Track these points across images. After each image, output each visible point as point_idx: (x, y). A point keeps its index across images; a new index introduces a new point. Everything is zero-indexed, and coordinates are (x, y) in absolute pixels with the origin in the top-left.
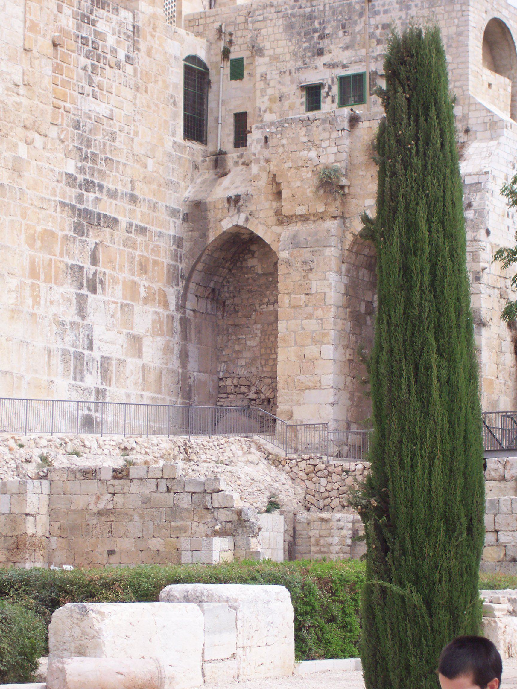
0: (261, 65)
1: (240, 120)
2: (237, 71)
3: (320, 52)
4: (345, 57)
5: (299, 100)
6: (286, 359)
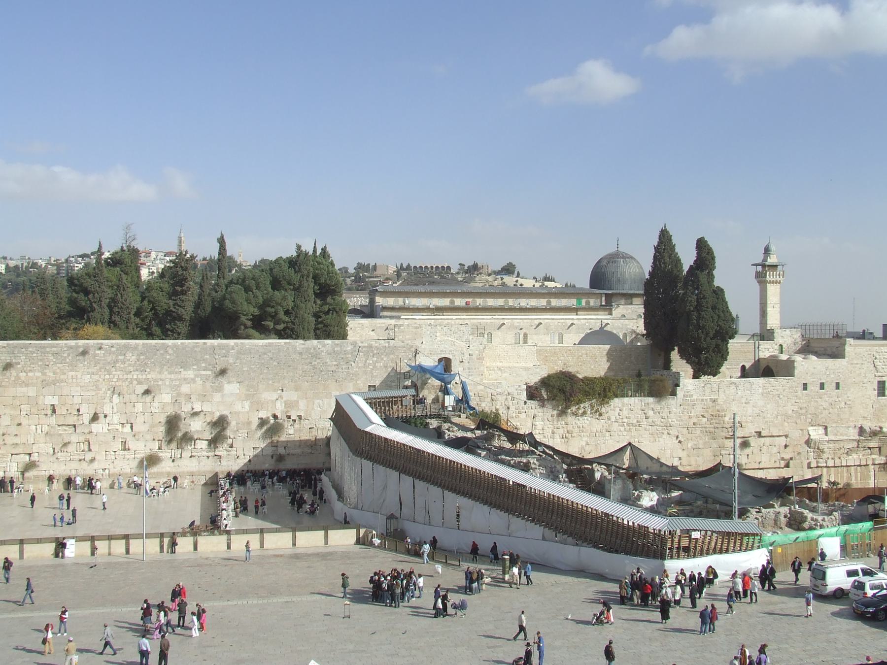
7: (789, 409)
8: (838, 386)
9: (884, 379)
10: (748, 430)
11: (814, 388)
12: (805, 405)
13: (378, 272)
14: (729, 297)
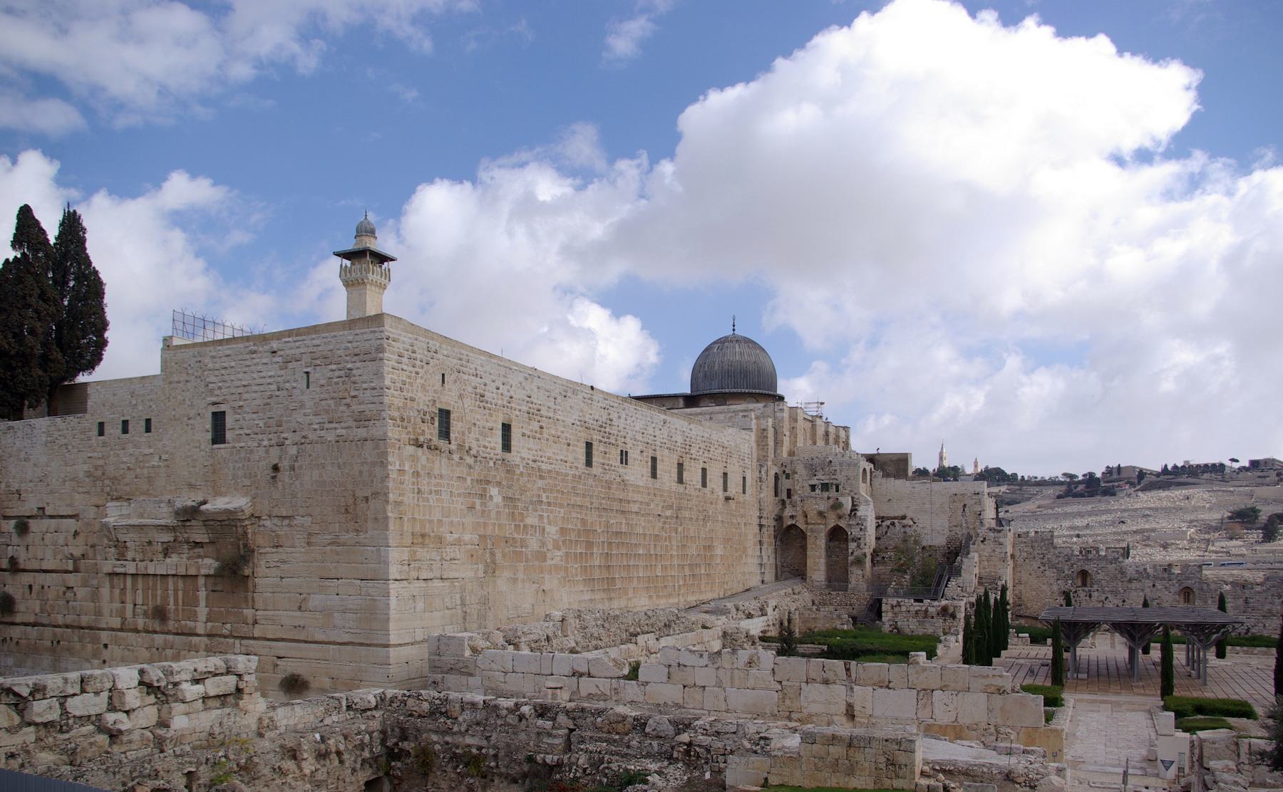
0: (796, 476)
1: (789, 491)
2: (788, 477)
5: (808, 489)
6: (810, 562)
7: (81, 469)
9: (222, 408)
10: (29, 507)
11: (113, 431)
12: (101, 462)
13: (1123, 475)
14: (107, 299)
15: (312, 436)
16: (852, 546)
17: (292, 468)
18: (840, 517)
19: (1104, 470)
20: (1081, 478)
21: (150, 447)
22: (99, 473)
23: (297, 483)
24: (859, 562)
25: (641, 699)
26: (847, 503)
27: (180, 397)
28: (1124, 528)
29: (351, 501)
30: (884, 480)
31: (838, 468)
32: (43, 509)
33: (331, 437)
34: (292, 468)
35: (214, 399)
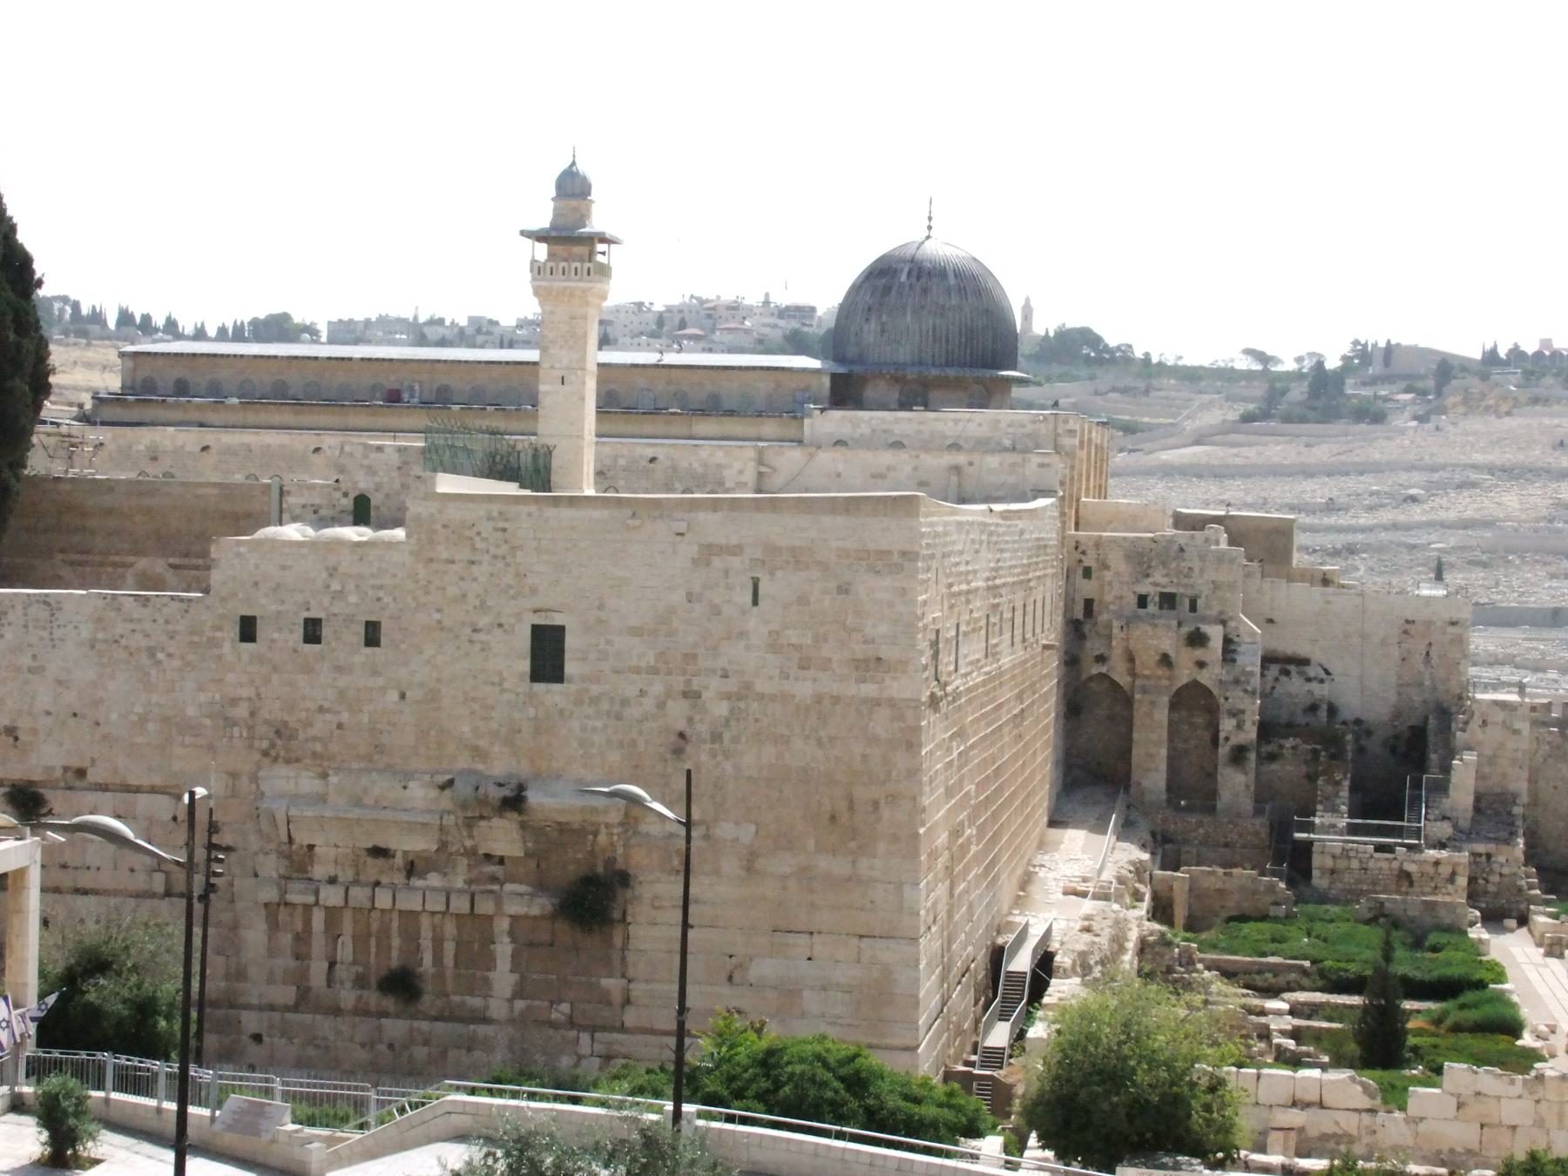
0: (1108, 575)
1: (1089, 604)
3: (1148, 576)
4: (1164, 581)
5: (1134, 600)
8: (372, 635)
9: (557, 620)
11: (280, 637)
12: (246, 692)
15: (761, 686)
16: (1227, 725)
17: (716, 737)
18: (1201, 665)
19: (1346, 349)
20: (1289, 366)
21: (375, 673)
22: (242, 711)
23: (728, 766)
24: (1238, 756)
25: (1410, 1142)
26: (1215, 633)
27: (453, 591)
28: (1417, 513)
29: (842, 806)
30: (1267, 584)
31: (1196, 565)
32: (81, 773)
33: (803, 689)
34: (716, 737)
35: (538, 603)
